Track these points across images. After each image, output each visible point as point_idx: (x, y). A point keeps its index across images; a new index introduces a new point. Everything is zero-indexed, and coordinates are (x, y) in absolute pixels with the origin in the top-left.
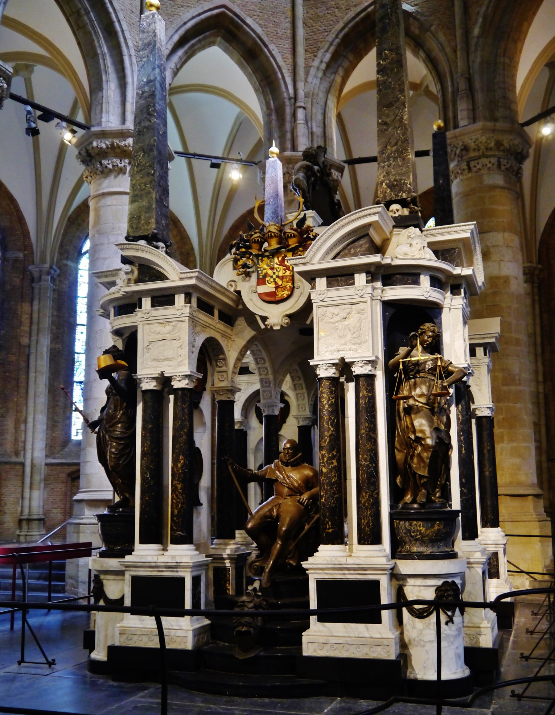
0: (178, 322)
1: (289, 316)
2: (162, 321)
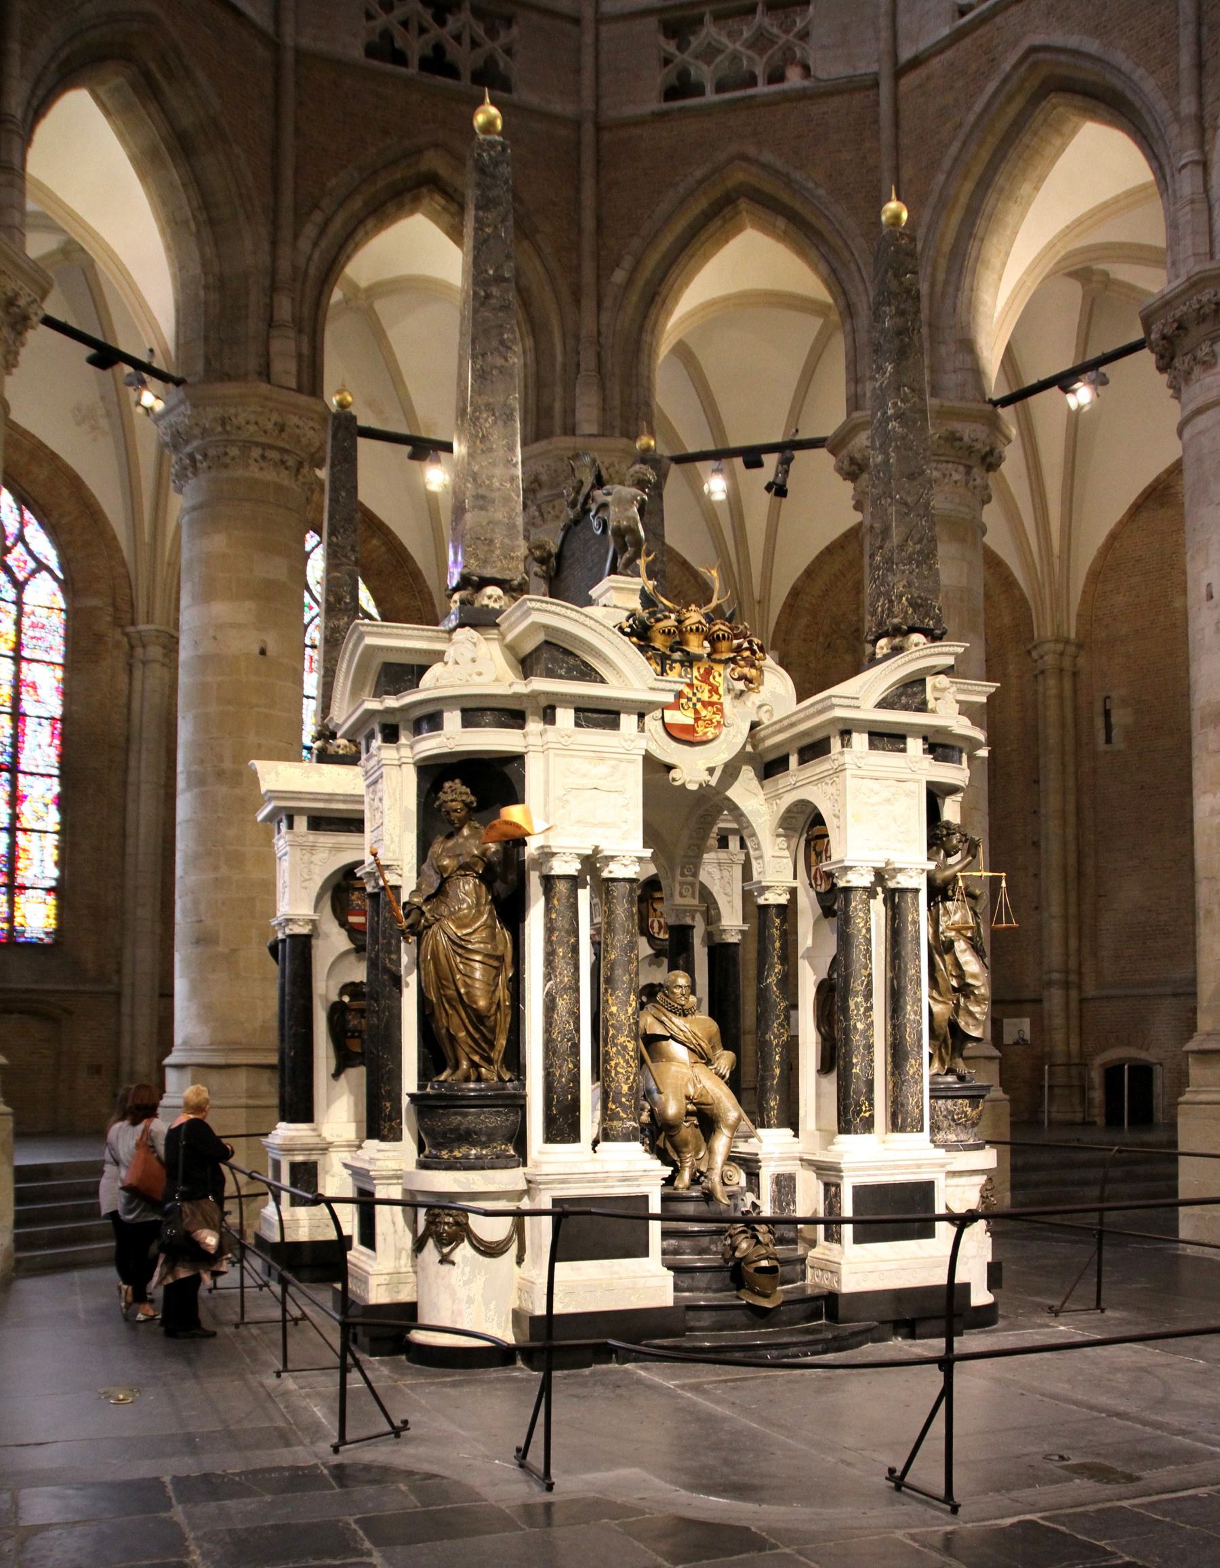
0: (621, 761)
2: (592, 754)
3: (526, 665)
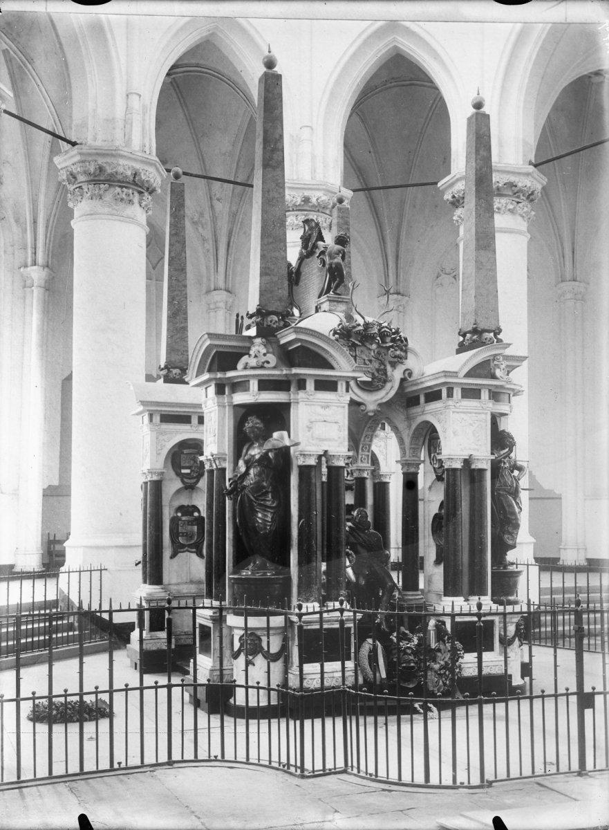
1: (380, 405)
3: (289, 356)
